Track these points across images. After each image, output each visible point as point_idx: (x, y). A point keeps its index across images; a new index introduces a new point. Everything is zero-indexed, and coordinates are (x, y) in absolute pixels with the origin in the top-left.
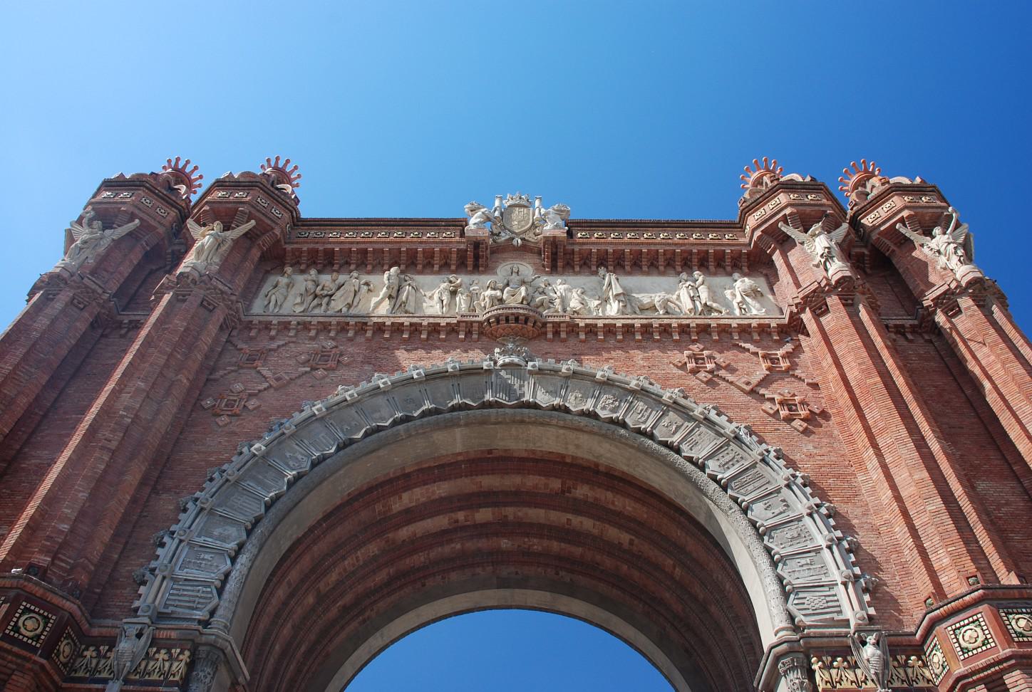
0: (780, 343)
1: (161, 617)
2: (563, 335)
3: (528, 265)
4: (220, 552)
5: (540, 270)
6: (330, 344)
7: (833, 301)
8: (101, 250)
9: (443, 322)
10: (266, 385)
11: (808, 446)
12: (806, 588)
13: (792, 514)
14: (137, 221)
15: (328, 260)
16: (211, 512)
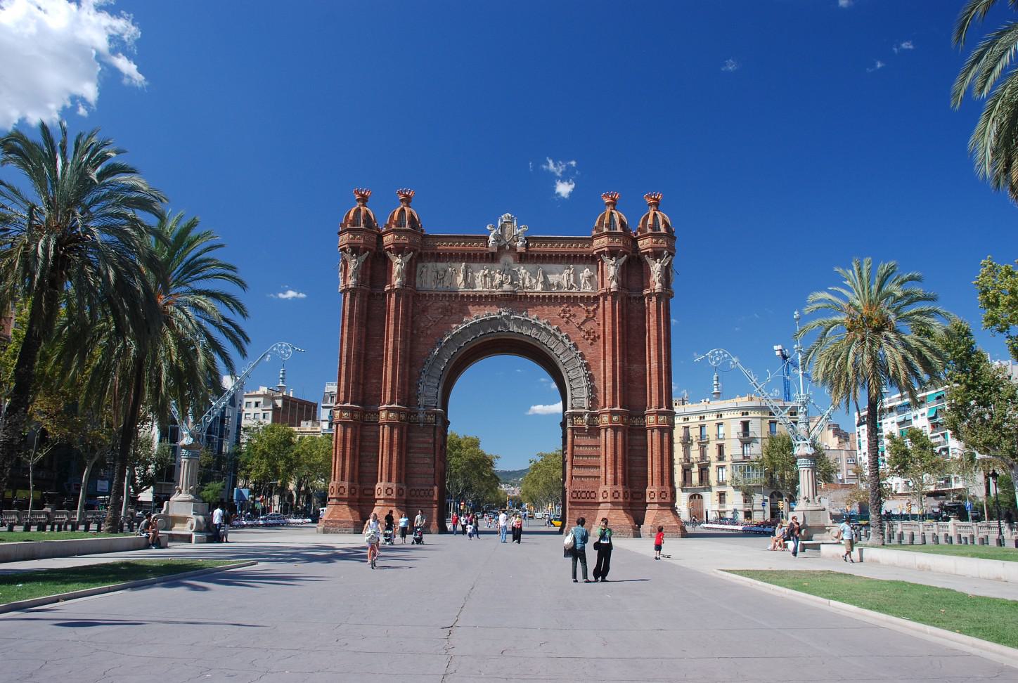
0: (593, 304)
1: (425, 406)
2: (522, 300)
3: (511, 257)
4: (434, 387)
5: (515, 261)
6: (447, 304)
7: (609, 298)
8: (360, 268)
9: (483, 294)
10: (430, 324)
11: (590, 350)
12: (578, 398)
13: (579, 376)
14: (368, 252)
15: (438, 257)
16: (428, 375)
